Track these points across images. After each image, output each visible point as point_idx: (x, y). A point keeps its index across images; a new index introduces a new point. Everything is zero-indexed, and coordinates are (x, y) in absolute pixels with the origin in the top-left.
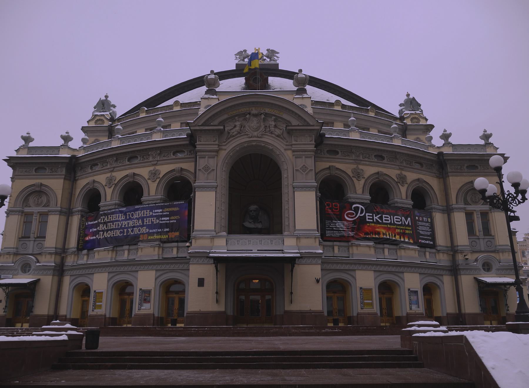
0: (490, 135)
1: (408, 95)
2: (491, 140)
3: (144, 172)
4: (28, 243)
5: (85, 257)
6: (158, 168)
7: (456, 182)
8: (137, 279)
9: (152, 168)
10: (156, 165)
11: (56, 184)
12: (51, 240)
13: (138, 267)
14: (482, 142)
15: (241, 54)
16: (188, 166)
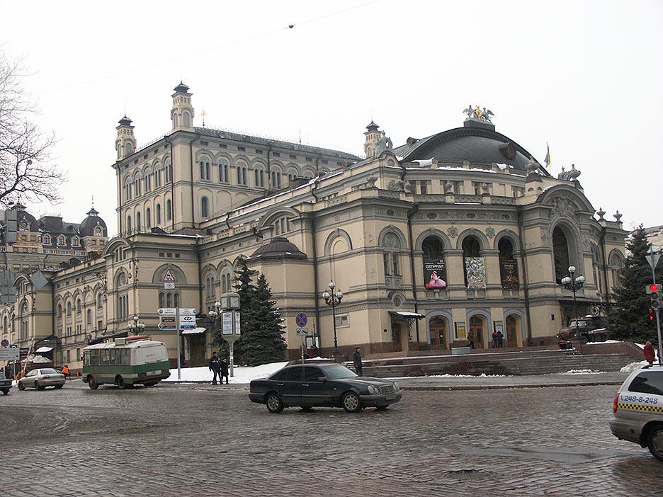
0: (621, 216)
1: (563, 169)
2: (621, 219)
3: (482, 228)
4: (390, 280)
5: (437, 295)
6: (492, 227)
7: (608, 248)
8: (490, 314)
9: (488, 226)
10: (490, 224)
11: (403, 227)
12: (407, 280)
13: (490, 305)
14: (615, 220)
15: (469, 110)
16: (515, 229)
